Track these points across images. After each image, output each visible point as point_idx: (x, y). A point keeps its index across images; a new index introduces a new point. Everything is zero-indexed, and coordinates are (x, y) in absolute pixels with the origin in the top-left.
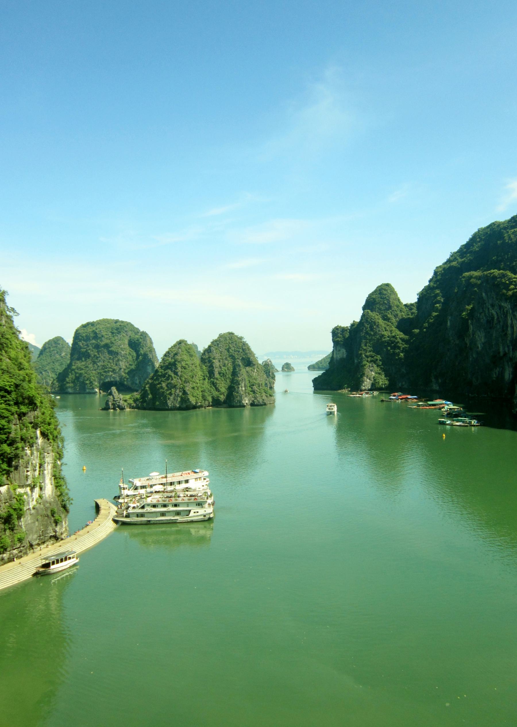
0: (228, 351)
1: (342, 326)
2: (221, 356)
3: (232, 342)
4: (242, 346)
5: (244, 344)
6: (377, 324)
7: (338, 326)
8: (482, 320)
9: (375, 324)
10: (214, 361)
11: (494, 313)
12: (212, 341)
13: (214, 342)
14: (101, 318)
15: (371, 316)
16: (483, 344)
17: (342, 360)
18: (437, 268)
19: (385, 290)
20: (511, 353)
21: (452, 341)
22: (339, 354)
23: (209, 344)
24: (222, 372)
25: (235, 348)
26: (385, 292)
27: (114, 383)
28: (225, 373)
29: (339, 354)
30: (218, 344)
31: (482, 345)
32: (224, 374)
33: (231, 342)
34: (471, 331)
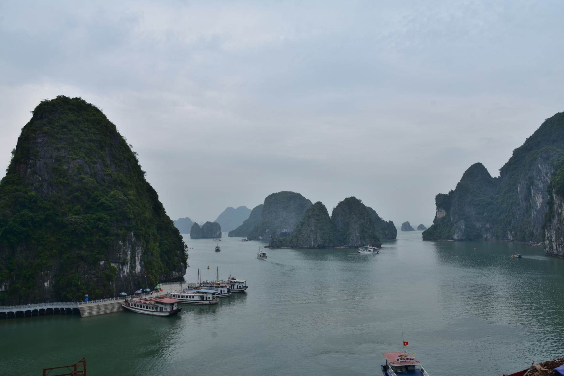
8: (540, 185)
11: (549, 180)
14: (281, 191)
17: (443, 218)
18: (515, 149)
21: (521, 203)
22: (441, 214)
27: (288, 233)
29: (441, 214)
31: (541, 205)
34: (532, 194)
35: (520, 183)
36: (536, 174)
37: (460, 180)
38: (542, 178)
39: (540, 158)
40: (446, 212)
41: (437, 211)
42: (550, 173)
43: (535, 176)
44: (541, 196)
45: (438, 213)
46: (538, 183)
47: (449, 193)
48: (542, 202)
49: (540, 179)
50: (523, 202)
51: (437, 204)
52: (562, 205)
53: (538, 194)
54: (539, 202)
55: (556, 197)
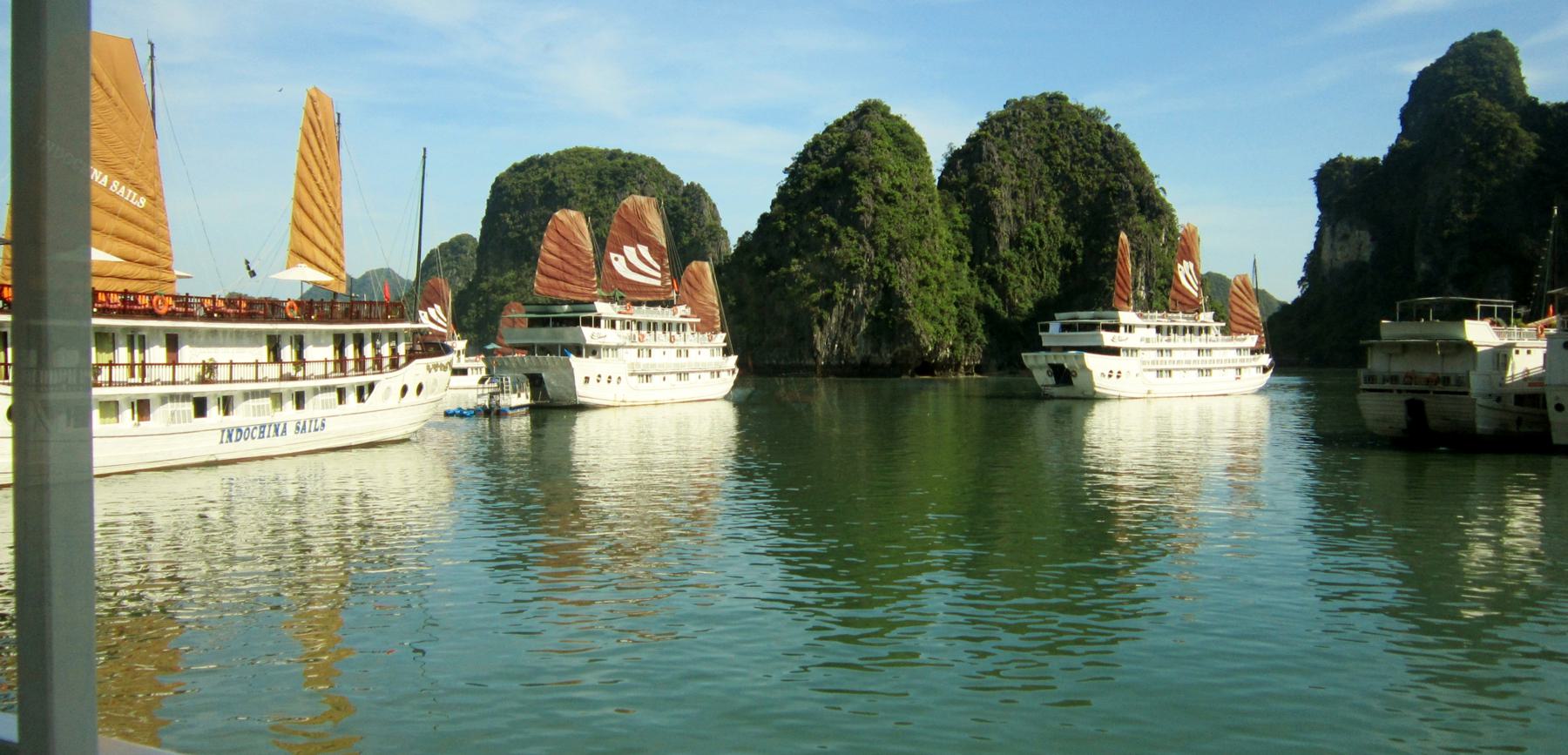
0: (1048, 160)
1: (1357, 156)
2: (1019, 176)
3: (1062, 126)
4: (1103, 142)
5: (1110, 134)
6: (1509, 138)
7: (1340, 156)
9: (1503, 135)
10: (996, 192)
12: (983, 118)
13: (995, 123)
15: (1487, 110)
17: (1356, 270)
19: (1489, 49)
23: (972, 128)
24: (1027, 238)
25: (1077, 150)
26: (1492, 56)
28: (1037, 244)
30: (1008, 131)
32: (1031, 245)
33: (1057, 125)
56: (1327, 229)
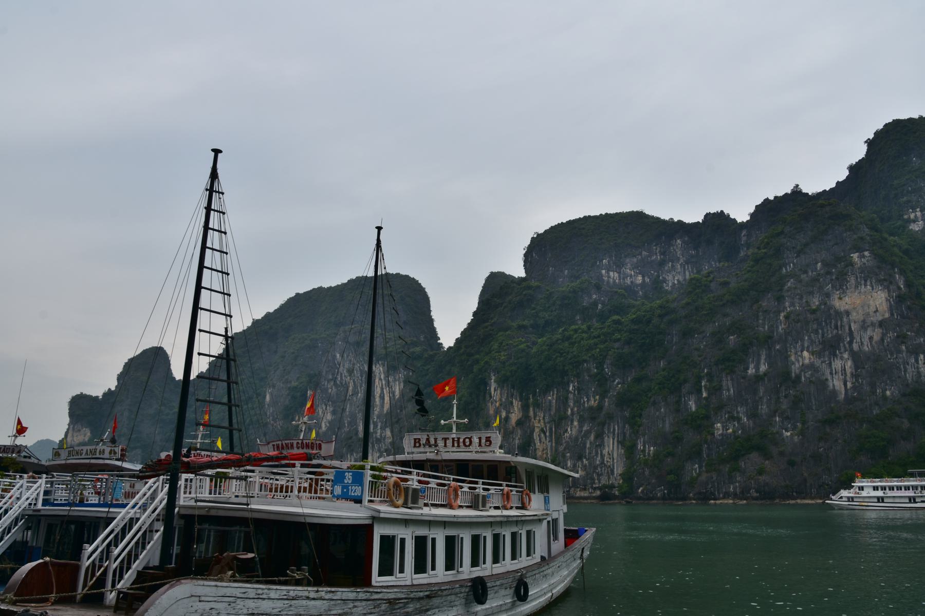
16: (330, 423)
20: (379, 431)
21: (272, 422)
31: (328, 425)
35: (274, 386)
36: (328, 370)
37: (119, 373)
38: (336, 378)
39: (340, 343)
40: (91, 433)
41: (68, 430)
42: (360, 369)
43: (324, 373)
44: (331, 409)
45: (70, 435)
46: (327, 385)
47: (105, 395)
48: (332, 420)
49: (332, 380)
50: (276, 422)
51: (71, 415)
52: (512, 403)
53: (326, 405)
54: (325, 421)
55: (495, 388)
56: (71, 426)
